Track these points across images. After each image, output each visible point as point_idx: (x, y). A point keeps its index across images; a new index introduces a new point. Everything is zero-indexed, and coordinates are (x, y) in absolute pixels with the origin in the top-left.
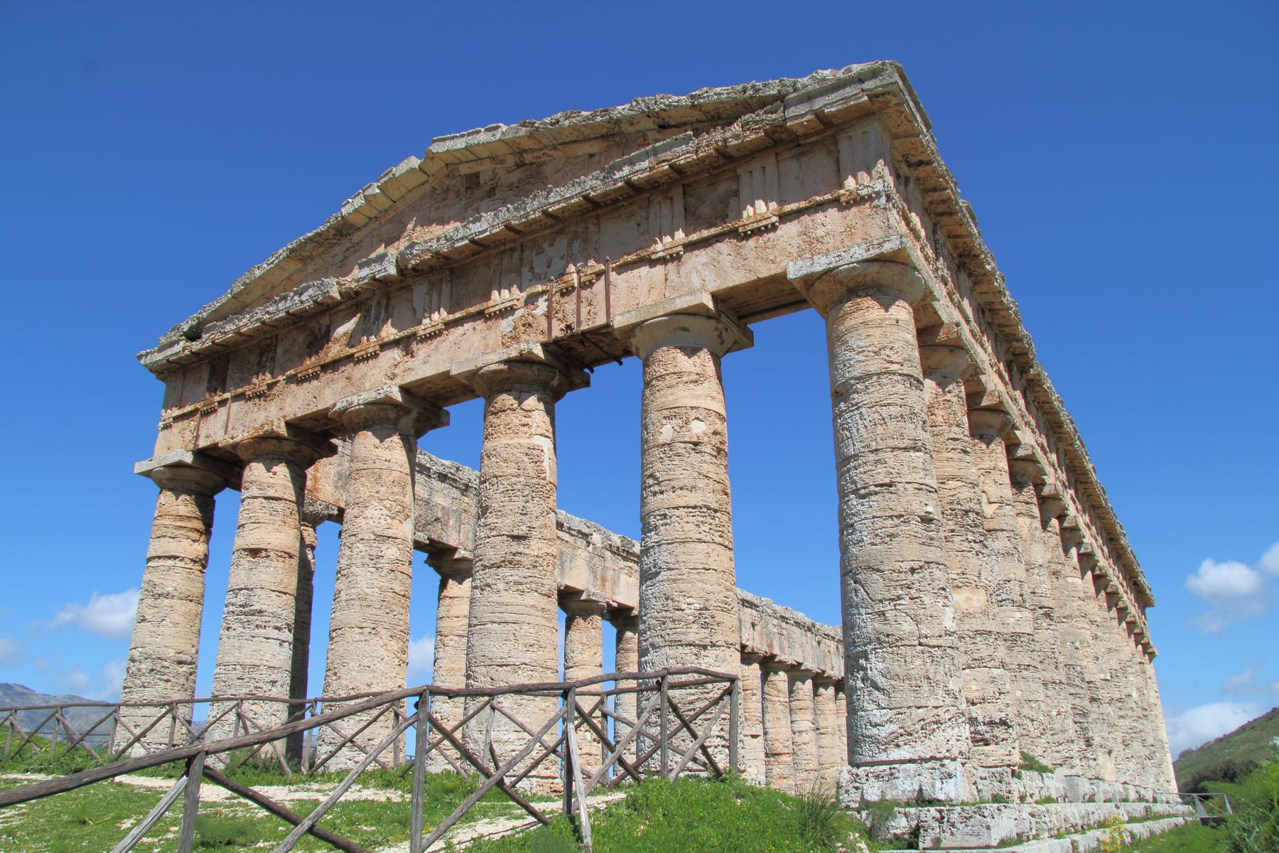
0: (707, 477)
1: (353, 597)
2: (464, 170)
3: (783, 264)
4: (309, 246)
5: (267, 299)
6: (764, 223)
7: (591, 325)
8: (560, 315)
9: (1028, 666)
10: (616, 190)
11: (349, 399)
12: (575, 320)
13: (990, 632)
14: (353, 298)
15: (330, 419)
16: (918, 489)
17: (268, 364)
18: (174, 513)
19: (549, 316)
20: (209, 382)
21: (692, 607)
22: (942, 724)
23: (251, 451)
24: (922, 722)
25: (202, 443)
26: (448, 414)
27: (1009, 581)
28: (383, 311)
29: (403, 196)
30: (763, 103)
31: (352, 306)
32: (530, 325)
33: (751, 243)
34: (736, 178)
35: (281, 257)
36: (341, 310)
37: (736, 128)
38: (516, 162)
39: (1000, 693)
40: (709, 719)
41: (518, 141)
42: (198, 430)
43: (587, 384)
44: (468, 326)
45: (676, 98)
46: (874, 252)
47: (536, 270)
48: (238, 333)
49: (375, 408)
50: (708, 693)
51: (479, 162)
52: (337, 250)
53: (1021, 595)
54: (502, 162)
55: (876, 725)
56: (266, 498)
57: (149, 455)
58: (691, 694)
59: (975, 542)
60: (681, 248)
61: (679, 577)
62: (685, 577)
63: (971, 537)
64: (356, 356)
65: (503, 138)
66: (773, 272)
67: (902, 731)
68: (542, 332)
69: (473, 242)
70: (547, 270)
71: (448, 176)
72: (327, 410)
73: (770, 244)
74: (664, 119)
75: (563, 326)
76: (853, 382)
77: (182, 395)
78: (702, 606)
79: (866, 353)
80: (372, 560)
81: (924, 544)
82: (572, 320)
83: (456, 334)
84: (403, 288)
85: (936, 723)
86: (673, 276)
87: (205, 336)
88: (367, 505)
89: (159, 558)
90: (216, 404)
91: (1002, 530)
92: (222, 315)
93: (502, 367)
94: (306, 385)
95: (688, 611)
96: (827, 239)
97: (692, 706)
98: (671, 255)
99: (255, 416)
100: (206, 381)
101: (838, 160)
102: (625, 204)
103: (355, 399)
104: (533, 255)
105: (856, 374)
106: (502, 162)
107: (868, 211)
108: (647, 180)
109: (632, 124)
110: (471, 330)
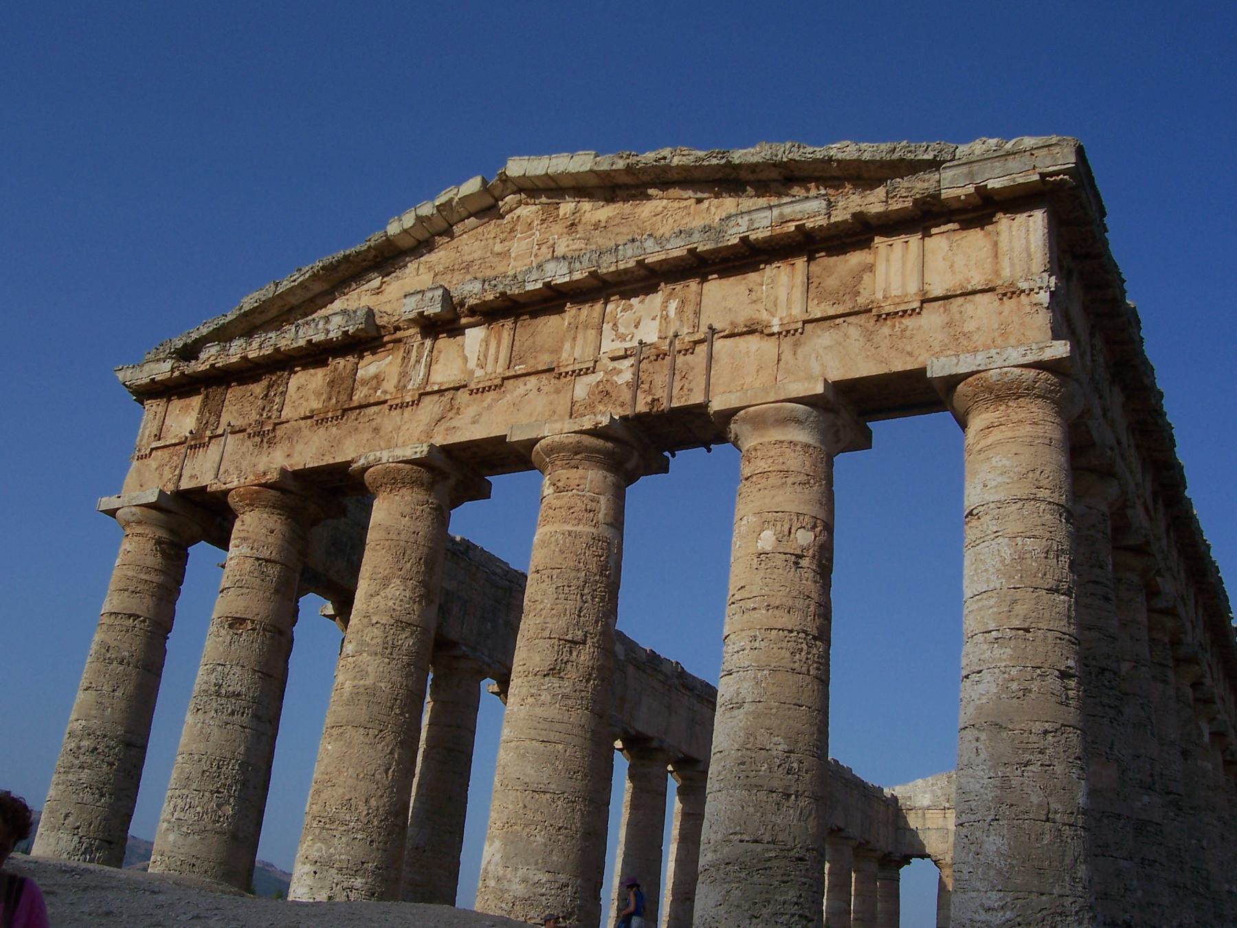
0: (808, 597)
1: (362, 690)
3: (921, 359)
4: (343, 267)
6: (903, 307)
7: (682, 403)
8: (646, 386)
9: (1154, 861)
10: (728, 247)
11: (378, 454)
12: (665, 395)
13: (1119, 815)
15: (349, 474)
16: (1060, 639)
17: (277, 400)
19: (636, 385)
20: (201, 412)
21: (780, 748)
22: (1067, 916)
24: (1044, 912)
25: (185, 485)
26: (490, 483)
27: (1138, 757)
30: (913, 167)
32: (608, 393)
33: (885, 330)
35: (307, 275)
37: (881, 192)
39: (1126, 890)
40: (787, 882)
41: (613, 174)
43: (664, 469)
45: (810, 149)
46: (1031, 358)
47: (622, 330)
49: (408, 466)
50: (789, 850)
53: (1151, 775)
55: (988, 910)
56: (258, 559)
57: (116, 490)
58: (767, 850)
59: (1110, 707)
61: (768, 711)
62: (774, 711)
63: (1106, 701)
64: (389, 403)
65: (596, 168)
66: (909, 367)
67: (1019, 919)
68: (623, 405)
69: (547, 285)
70: (635, 331)
72: (348, 464)
73: (908, 333)
74: (792, 171)
75: (649, 399)
76: (992, 506)
78: (790, 748)
79: (1011, 474)
80: (386, 648)
81: (1061, 703)
82: (659, 393)
83: (516, 394)
85: (1061, 914)
86: (787, 356)
87: (203, 356)
88: (387, 582)
91: (1134, 695)
92: (222, 335)
93: (575, 438)
94: (322, 431)
95: (774, 753)
96: (975, 337)
97: (768, 864)
99: (254, 460)
100: (197, 411)
101: (996, 244)
102: (737, 264)
103: (385, 456)
104: (619, 309)
105: (997, 498)
107: (1028, 309)
108: (766, 241)
109: (753, 172)
110: (535, 390)
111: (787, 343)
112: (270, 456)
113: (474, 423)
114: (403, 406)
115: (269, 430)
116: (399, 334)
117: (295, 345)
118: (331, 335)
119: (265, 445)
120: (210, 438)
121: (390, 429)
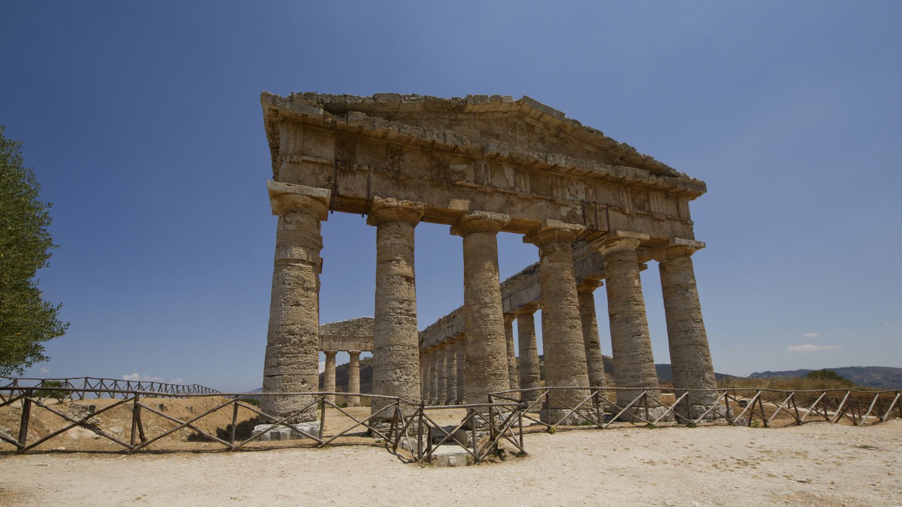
2: (528, 119)
5: (389, 117)
11: (484, 213)
23: (402, 215)
28: (489, 171)
29: (493, 112)
31: (466, 158)
33: (656, 223)
34: (648, 195)
36: (459, 157)
38: (555, 133)
44: (544, 203)
51: (537, 121)
52: (446, 116)
54: (548, 129)
60: (634, 213)
64: (478, 189)
71: (517, 117)
75: (590, 224)
77: (303, 145)
82: (594, 223)
84: (499, 165)
86: (630, 222)
98: (631, 214)
104: (569, 184)
106: (548, 129)
110: (545, 206)
112: (408, 193)
113: (522, 212)
115: (403, 179)
119: (402, 188)
121: (480, 202)
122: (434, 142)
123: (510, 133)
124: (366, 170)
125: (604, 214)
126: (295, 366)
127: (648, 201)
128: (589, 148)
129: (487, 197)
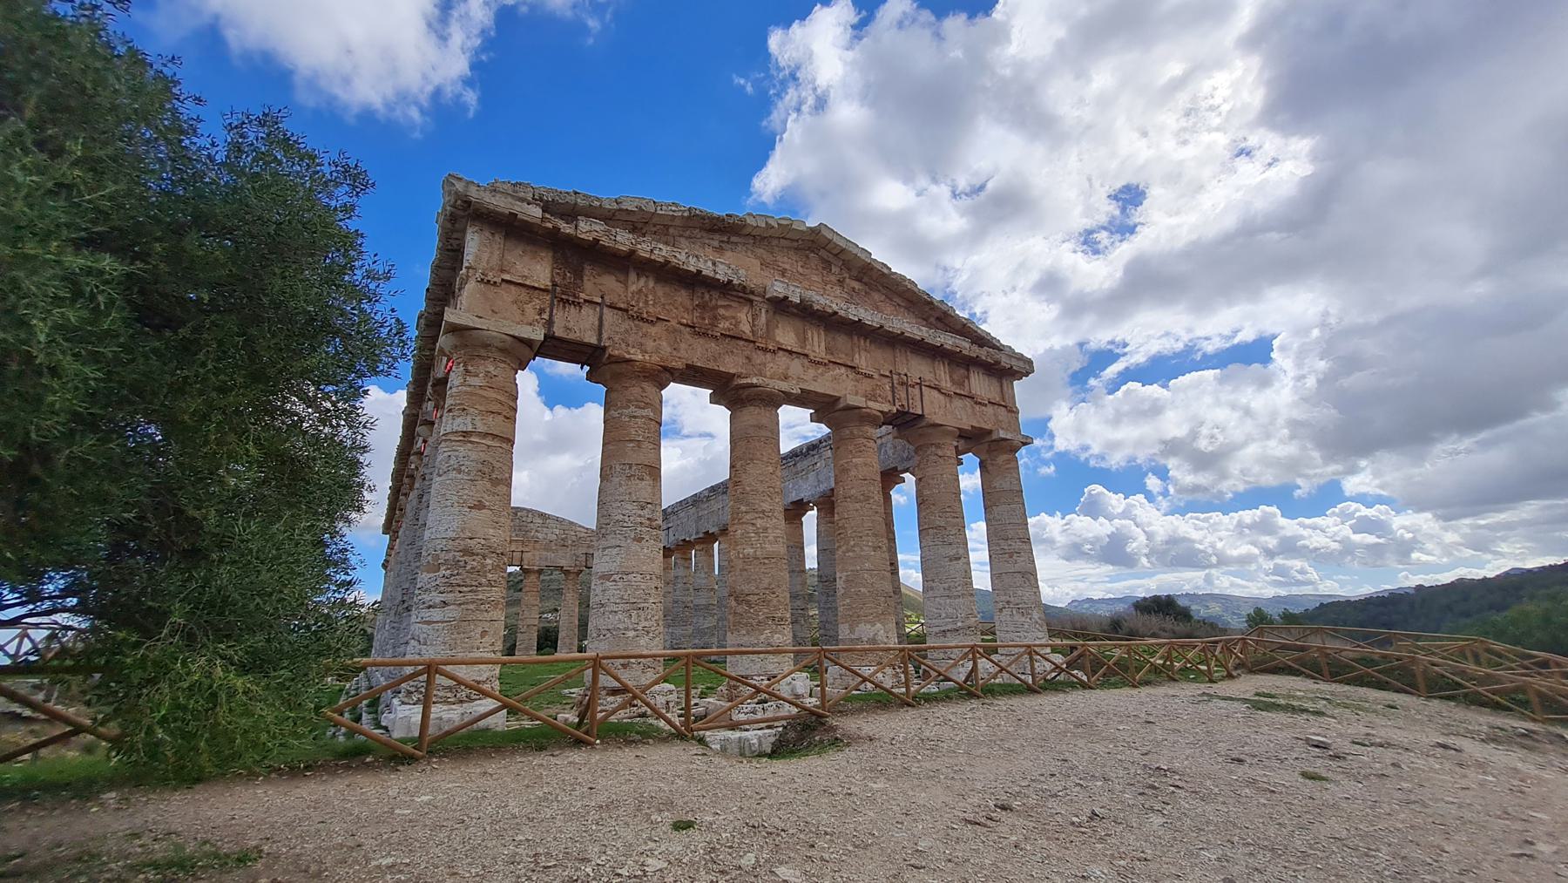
14: (744, 293)
18: (509, 390)
33: (977, 407)
34: (968, 370)
42: (551, 315)
44: (843, 370)
48: (632, 252)
86: (948, 405)
89: (494, 436)
90: (582, 301)
94: (702, 341)
111: (948, 399)
114: (765, 350)
116: (751, 297)
117: (685, 267)
118: (718, 276)
120: (585, 301)
122: (699, 272)
123: (800, 270)
124: (597, 303)
125: (916, 391)
126: (472, 607)
127: (968, 378)
128: (898, 300)
129: (769, 355)
